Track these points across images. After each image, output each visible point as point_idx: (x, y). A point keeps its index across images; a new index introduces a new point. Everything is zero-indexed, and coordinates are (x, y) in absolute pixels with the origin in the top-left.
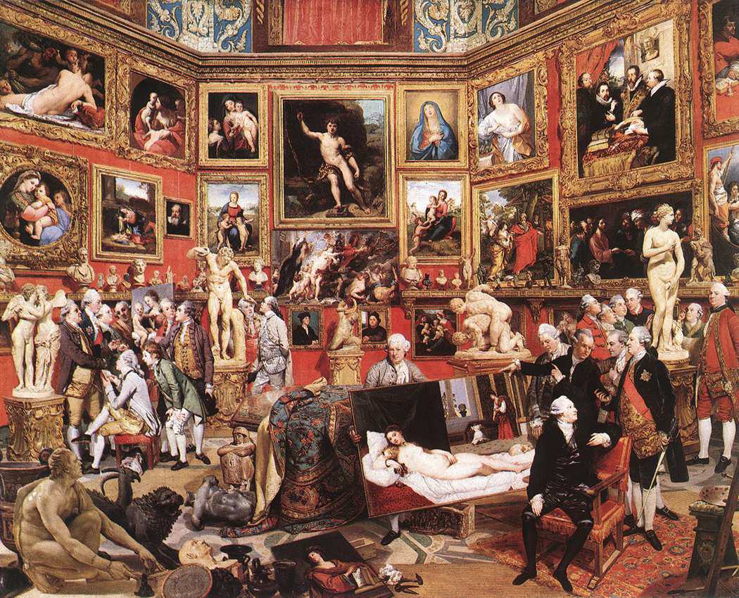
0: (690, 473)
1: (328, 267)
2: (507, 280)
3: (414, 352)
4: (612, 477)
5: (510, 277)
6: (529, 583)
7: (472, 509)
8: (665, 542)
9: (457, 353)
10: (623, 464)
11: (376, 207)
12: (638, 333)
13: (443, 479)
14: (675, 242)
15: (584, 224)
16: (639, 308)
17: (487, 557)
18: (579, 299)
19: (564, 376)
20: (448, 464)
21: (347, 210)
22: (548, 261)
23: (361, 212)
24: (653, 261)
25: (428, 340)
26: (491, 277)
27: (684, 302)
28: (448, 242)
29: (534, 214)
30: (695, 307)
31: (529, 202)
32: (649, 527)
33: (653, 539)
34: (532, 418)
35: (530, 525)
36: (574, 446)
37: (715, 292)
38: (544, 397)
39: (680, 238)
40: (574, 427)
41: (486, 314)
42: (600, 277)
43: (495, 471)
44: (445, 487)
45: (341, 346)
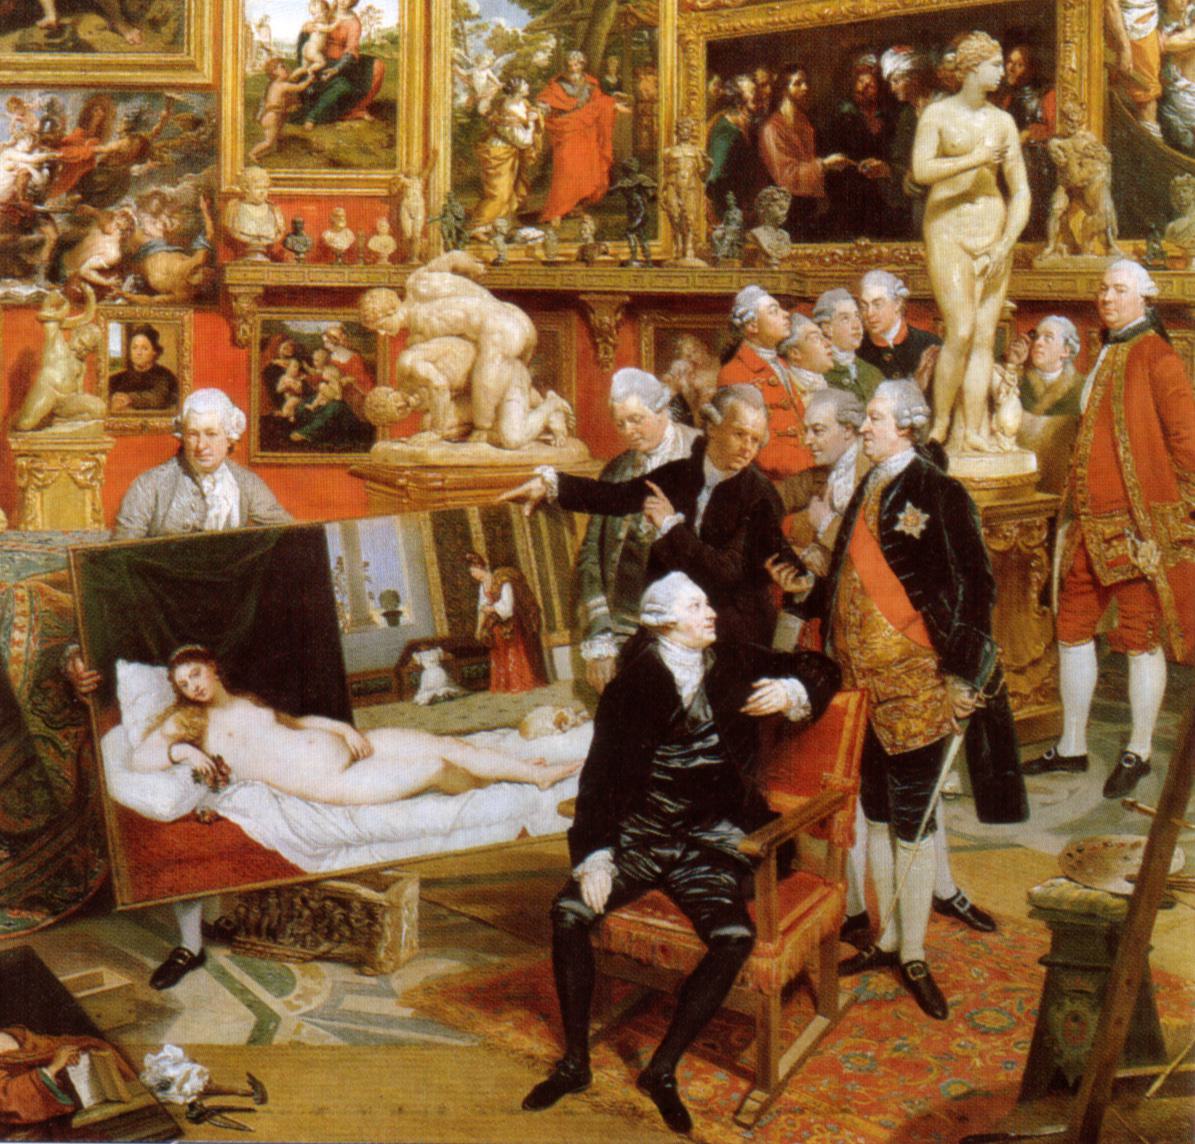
0: (1033, 800)
1: (14, 196)
2: (525, 240)
3: (254, 439)
4: (803, 809)
5: (530, 232)
6: (567, 1101)
7: (411, 891)
9: (381, 446)
10: (841, 773)
11: (155, 24)
12: (892, 398)
13: (331, 803)
14: (1003, 140)
15: (746, 85)
17: (454, 1027)
18: (723, 303)
19: (680, 517)
20: (345, 758)
21: (74, 33)
22: (641, 189)
23: (108, 34)
24: (940, 193)
25: (296, 408)
26: (480, 230)
27: (1029, 311)
28: (358, 126)
29: (606, 55)
30: (1058, 330)
32: (913, 952)
33: (925, 993)
34: (588, 633)
36: (704, 714)
37: (1116, 286)
38: (623, 577)
40: (705, 661)
41: (461, 336)
42: (786, 235)
43: (479, 782)
44: (335, 824)
45: (48, 420)
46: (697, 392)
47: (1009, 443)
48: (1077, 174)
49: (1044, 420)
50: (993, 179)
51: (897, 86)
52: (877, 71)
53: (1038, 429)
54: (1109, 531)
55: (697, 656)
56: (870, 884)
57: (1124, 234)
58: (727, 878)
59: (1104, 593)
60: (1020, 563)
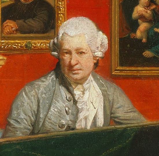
3: (115, 59)
25: (148, 31)
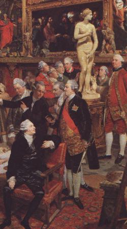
0: (100, 165)
4: (54, 167)
8: (85, 205)
10: (62, 159)
12: (70, 83)
16: (71, 68)
18: (37, 64)
19: (28, 108)
22: (19, 42)
24: (80, 41)
29: (12, 14)
30: (104, 69)
31: (9, 8)
32: (77, 196)
33: (79, 204)
34: (10, 132)
35: (9, 194)
36: (33, 148)
39: (96, 28)
40: (33, 137)
46: (31, 83)
47: (94, 92)
48: (108, 37)
49: (101, 87)
50: (90, 38)
51: (71, 20)
52: (67, 16)
53: (100, 89)
54: (115, 109)
55: (32, 137)
56: (67, 182)
57: (117, 49)
58: (38, 182)
59: (114, 122)
60: (97, 116)
